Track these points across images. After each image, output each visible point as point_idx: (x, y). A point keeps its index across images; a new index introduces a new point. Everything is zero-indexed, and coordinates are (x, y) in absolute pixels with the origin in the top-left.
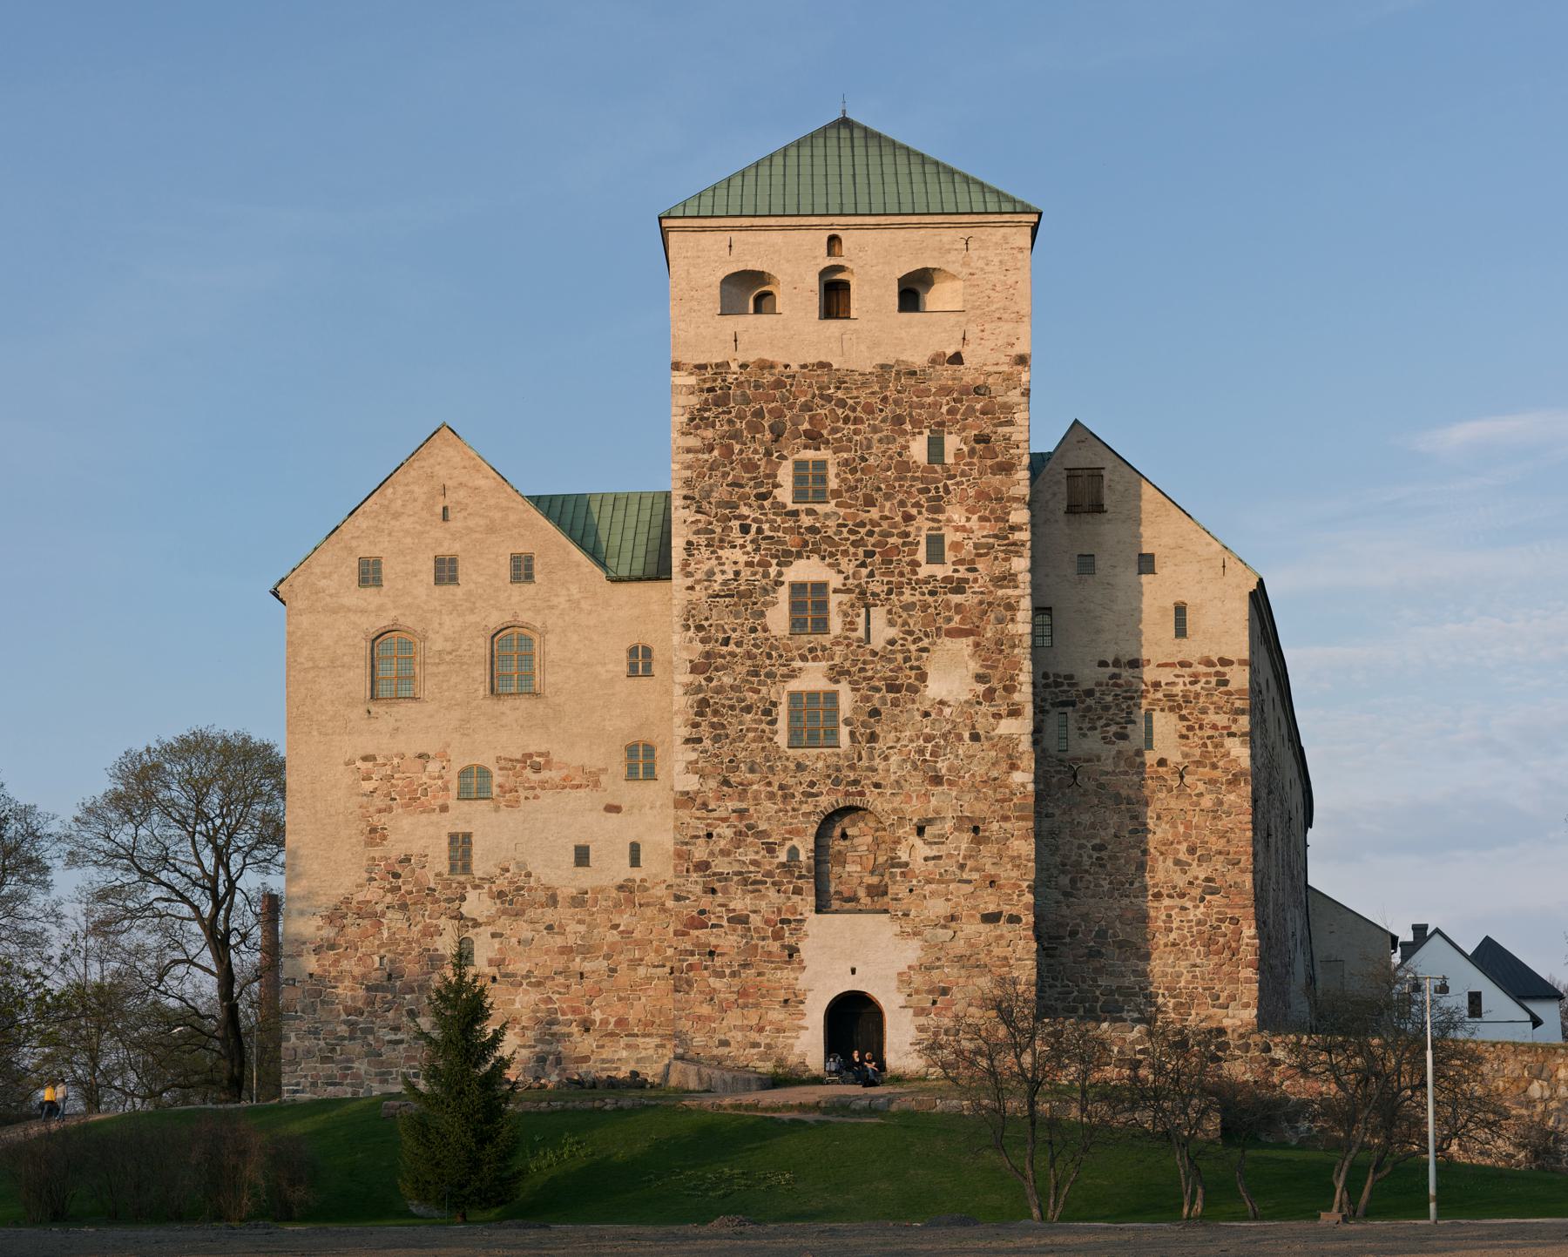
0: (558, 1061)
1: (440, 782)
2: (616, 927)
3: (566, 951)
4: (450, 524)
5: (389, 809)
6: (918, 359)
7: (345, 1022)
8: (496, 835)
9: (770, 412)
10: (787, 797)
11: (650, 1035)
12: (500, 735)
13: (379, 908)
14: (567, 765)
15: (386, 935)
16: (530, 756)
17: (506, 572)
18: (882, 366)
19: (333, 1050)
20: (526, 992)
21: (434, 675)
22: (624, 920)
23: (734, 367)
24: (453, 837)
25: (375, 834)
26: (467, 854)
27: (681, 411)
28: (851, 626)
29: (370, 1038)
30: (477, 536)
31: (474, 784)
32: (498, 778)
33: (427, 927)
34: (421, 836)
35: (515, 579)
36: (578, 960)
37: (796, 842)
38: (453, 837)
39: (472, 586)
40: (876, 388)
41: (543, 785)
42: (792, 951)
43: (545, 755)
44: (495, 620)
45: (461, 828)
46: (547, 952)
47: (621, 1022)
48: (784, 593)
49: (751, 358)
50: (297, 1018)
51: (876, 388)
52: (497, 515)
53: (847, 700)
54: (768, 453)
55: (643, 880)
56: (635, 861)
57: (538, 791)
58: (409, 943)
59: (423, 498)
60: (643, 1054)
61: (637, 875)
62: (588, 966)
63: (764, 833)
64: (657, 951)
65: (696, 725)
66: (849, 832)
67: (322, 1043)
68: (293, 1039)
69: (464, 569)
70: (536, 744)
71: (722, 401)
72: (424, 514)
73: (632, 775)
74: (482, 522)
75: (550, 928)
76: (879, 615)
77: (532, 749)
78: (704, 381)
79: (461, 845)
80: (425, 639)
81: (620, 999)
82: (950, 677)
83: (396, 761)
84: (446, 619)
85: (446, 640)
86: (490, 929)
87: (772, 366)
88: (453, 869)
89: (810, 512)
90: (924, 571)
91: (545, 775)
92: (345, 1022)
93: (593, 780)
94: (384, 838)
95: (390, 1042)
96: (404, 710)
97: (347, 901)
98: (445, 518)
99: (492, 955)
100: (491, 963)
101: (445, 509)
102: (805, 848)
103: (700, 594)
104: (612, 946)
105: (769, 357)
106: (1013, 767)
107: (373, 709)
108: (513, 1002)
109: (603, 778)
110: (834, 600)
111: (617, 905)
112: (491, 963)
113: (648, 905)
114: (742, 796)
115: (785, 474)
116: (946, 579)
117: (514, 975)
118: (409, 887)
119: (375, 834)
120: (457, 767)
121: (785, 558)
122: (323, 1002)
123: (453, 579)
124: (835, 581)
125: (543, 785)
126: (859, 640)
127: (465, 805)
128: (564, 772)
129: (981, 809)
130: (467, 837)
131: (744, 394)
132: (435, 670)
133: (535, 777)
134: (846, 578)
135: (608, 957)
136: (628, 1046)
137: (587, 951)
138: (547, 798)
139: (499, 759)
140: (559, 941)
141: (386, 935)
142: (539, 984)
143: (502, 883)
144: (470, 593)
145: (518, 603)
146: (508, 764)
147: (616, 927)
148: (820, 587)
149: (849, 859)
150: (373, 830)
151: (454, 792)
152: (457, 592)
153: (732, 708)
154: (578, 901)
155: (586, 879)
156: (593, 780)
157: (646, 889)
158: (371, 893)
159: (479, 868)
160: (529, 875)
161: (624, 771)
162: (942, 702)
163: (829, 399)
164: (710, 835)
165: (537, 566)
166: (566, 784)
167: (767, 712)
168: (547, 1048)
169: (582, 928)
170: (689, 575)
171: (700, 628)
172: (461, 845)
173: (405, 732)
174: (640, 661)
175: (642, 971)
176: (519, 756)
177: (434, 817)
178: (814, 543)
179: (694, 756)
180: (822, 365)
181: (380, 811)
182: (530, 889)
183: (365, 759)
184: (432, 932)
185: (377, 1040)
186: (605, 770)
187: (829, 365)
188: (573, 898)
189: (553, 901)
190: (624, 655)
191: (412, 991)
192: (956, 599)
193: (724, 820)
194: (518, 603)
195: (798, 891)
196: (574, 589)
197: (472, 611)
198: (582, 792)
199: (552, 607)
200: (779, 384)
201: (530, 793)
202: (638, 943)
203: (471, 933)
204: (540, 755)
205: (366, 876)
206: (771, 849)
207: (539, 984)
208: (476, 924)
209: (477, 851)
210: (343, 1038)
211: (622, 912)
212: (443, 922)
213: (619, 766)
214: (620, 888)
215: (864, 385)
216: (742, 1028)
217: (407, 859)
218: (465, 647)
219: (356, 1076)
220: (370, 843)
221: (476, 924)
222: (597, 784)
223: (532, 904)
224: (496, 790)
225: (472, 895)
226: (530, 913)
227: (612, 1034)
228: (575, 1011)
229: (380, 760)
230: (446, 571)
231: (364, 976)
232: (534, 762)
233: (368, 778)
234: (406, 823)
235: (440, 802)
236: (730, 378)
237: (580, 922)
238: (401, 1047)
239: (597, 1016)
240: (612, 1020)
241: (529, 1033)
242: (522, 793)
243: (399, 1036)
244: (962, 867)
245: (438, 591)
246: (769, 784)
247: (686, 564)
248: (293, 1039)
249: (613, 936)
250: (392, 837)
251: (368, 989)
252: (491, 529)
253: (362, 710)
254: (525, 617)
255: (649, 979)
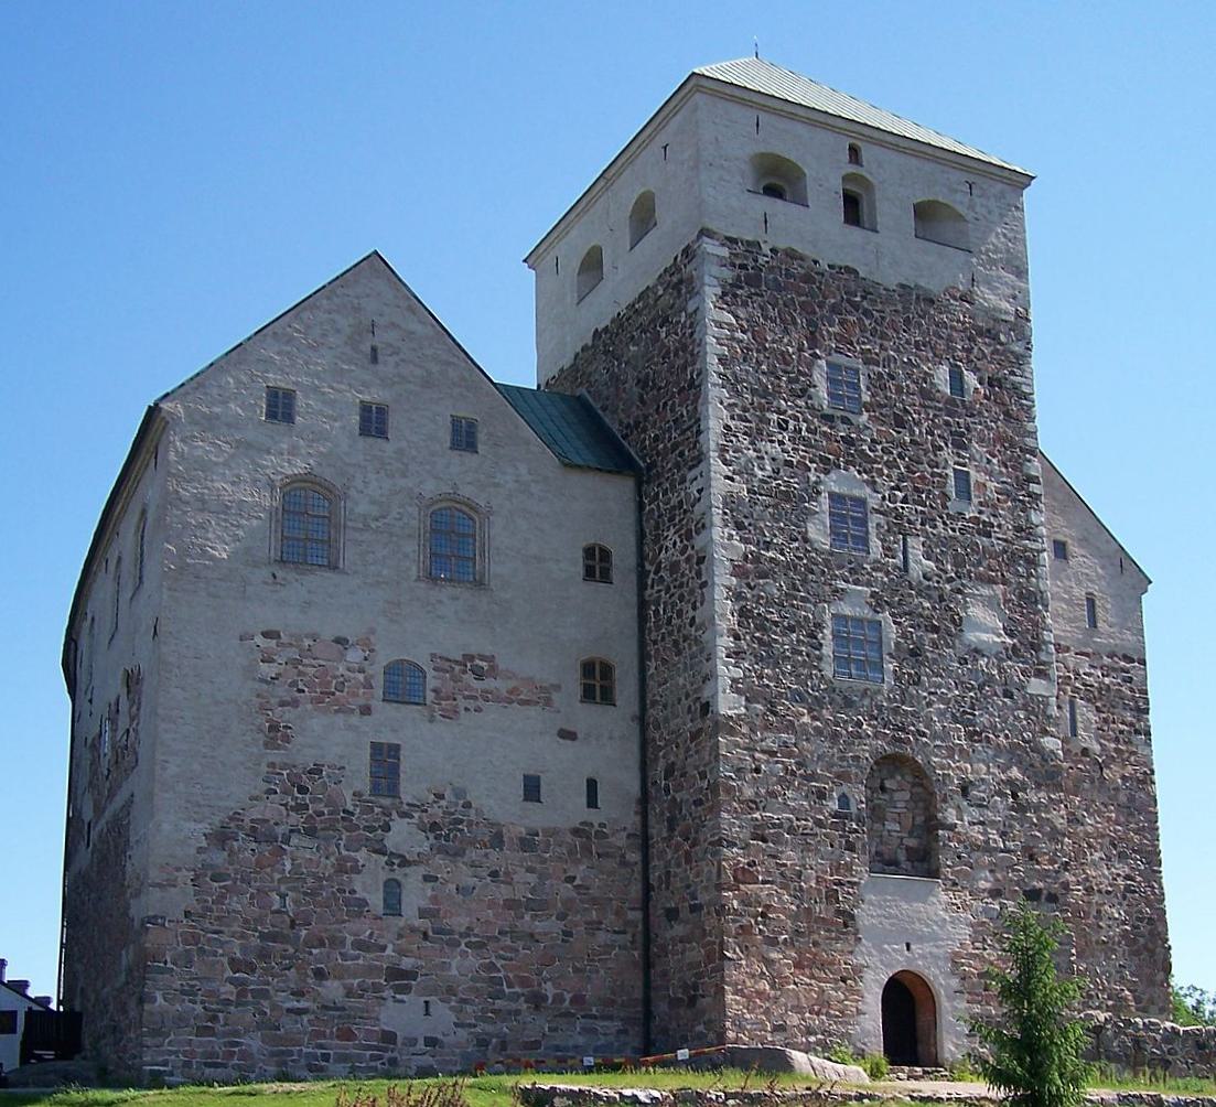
0: (503, 1046)
1: (361, 677)
2: (571, 879)
3: (510, 904)
4: (380, 367)
5: (295, 703)
6: (934, 286)
7: (231, 981)
8: (436, 754)
9: (802, 304)
10: (835, 736)
11: (610, 1018)
12: (436, 629)
13: (280, 830)
14: (511, 675)
15: (288, 867)
16: (471, 658)
17: (446, 437)
18: (903, 286)
19: (214, 1019)
20: (464, 954)
21: (360, 543)
22: (580, 871)
23: (766, 249)
24: (376, 748)
25: (276, 734)
26: (394, 771)
27: (715, 282)
28: (889, 551)
29: (266, 1003)
30: (412, 387)
31: (402, 684)
32: (432, 682)
33: (342, 860)
34: (335, 743)
35: (455, 446)
36: (527, 917)
37: (845, 789)
38: (376, 748)
39: (404, 444)
40: (899, 307)
41: (486, 696)
42: (849, 918)
43: (490, 659)
44: (430, 488)
45: (386, 737)
46: (492, 904)
47: (578, 1000)
48: (824, 499)
49: (781, 245)
50: (162, 971)
51: (899, 307)
52: (435, 368)
53: (891, 633)
54: (800, 350)
55: (602, 825)
56: (592, 802)
57: (480, 703)
58: (320, 879)
59: (348, 331)
60: (602, 1040)
61: (595, 817)
62: (539, 926)
63: (813, 777)
64: (617, 913)
65: (737, 637)
66: (888, 784)
67: (199, 1008)
68: (160, 1000)
69: (393, 420)
70: (479, 643)
71: (755, 281)
72: (348, 350)
73: (588, 695)
74: (418, 372)
75: (494, 874)
76: (916, 547)
77: (473, 650)
78: (736, 255)
79: (386, 760)
80: (346, 496)
81: (576, 970)
82: (985, 624)
83: (307, 642)
84: (372, 476)
85: (373, 502)
86: (422, 870)
87: (802, 258)
88: (375, 790)
89: (845, 420)
90: (954, 506)
91: (489, 683)
92: (231, 981)
93: (543, 697)
94: (287, 739)
95: (289, 1011)
96: (319, 580)
97: (236, 817)
98: (374, 359)
99: (424, 904)
100: (423, 913)
101: (374, 349)
102: (858, 795)
103: (740, 488)
104: (568, 903)
105: (799, 248)
106: (1045, 733)
107: (280, 574)
108: (445, 966)
109: (555, 696)
110: (875, 519)
111: (571, 853)
112: (423, 913)
113: (607, 855)
114: (790, 727)
115: (819, 377)
116: (976, 520)
117: (451, 932)
118: (321, 807)
119: (276, 734)
120: (384, 657)
121: (827, 466)
122: (202, 951)
123: (382, 433)
124: (873, 501)
125: (486, 696)
126: (896, 567)
127: (391, 709)
128: (511, 684)
129: (1015, 773)
130: (395, 750)
131: (775, 279)
132: (357, 535)
133: (476, 684)
134: (884, 498)
135: (562, 917)
136: (586, 1031)
137: (537, 906)
138: (492, 712)
139: (433, 656)
140: (504, 892)
141: (288, 867)
142: (480, 946)
143: (436, 812)
144: (400, 452)
145: (462, 474)
146: (444, 663)
147: (571, 879)
148: (861, 502)
149: (889, 815)
150: (274, 728)
151: (379, 692)
152: (388, 448)
153: (776, 624)
154: (527, 844)
155: (537, 817)
156: (543, 697)
157: (605, 836)
158: (269, 810)
159: (409, 791)
160: (468, 805)
161: (579, 691)
162: (976, 651)
163: (856, 306)
164: (757, 770)
165: (481, 436)
166: (509, 699)
167: (812, 636)
168: (490, 1028)
169: (532, 878)
170: (725, 462)
171: (739, 526)
172: (386, 760)
173: (319, 608)
174: (597, 564)
175: (602, 937)
176: (460, 658)
177: (355, 719)
178: (851, 453)
179: (739, 673)
180: (849, 270)
181: (283, 704)
182: (470, 824)
183: (266, 635)
184: (347, 868)
185: (274, 1007)
186: (557, 688)
187: (856, 272)
188: (522, 840)
189: (498, 840)
190: (580, 554)
191: (322, 944)
192: (982, 541)
193: (772, 754)
194: (462, 474)
195: (851, 847)
196: (523, 469)
197: (404, 476)
198: (533, 711)
199: (497, 485)
200: (808, 279)
201: (471, 704)
202: (594, 901)
203: (398, 874)
204: (483, 658)
205: (265, 786)
206: (821, 795)
207: (480, 946)
208: (405, 863)
209: (406, 765)
210: (228, 1002)
211: (578, 862)
212: (362, 855)
213: (573, 684)
214: (576, 832)
215: (888, 301)
216: (798, 1009)
217: (316, 770)
218: (394, 514)
219: (244, 1055)
220: (270, 744)
221: (405, 863)
222: (548, 702)
223: (472, 843)
224: (430, 696)
225: (400, 827)
226: (473, 854)
227: (567, 1014)
228: (524, 982)
229: (284, 639)
230: (374, 422)
231: (260, 920)
232: (477, 666)
233: (268, 660)
234: (317, 723)
235: (362, 702)
236: (762, 260)
237: (530, 870)
238: (305, 1018)
239: (549, 990)
240: (568, 997)
241: (469, 1008)
242: (462, 703)
243: (303, 1004)
244: (1003, 835)
245: (362, 443)
246: (814, 718)
247: (723, 450)
248: (160, 1000)
249: (567, 890)
250: (298, 740)
251: (263, 936)
252: (427, 383)
253: (265, 573)
254: (466, 491)
255: (608, 947)
